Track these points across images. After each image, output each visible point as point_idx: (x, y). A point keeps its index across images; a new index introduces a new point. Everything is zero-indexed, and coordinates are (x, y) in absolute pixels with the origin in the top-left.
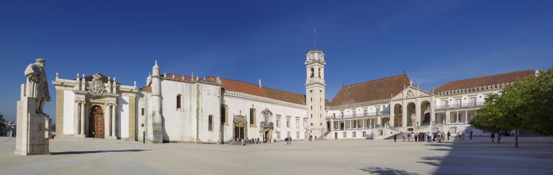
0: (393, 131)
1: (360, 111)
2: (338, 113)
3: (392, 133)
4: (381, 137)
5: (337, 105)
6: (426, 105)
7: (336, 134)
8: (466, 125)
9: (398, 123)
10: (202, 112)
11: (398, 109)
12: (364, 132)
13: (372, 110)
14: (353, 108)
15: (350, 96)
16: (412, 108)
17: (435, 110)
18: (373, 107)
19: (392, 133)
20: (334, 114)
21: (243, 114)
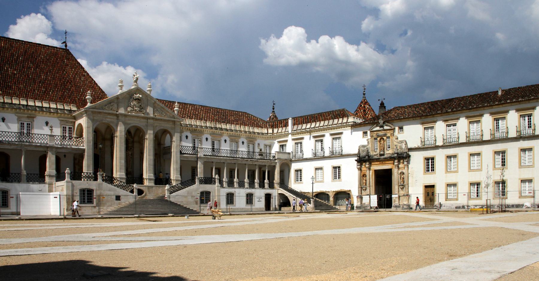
19: (118, 198)
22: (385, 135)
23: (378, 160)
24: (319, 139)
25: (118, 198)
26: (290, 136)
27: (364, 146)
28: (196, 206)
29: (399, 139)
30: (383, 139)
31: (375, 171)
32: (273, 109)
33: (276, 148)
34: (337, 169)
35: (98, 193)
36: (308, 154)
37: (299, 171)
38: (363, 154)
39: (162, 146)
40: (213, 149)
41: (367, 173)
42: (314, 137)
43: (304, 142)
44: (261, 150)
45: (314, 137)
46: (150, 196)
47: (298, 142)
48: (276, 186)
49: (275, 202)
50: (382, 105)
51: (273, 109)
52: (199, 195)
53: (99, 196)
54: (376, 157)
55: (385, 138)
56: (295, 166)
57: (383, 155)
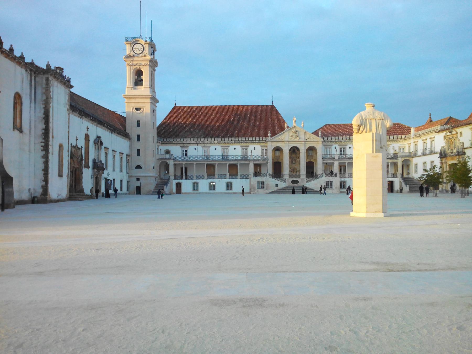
2: (176, 150)
7: (179, 186)
9: (277, 171)
10: (53, 137)
13: (235, 150)
18: (238, 147)
19: (277, 185)
20: (168, 152)
21: (79, 146)
22: (453, 138)
23: (450, 156)
25: (277, 185)
27: (443, 146)
29: (461, 141)
31: (451, 165)
33: (407, 150)
36: (420, 153)
37: (416, 164)
38: (442, 152)
41: (445, 165)
42: (423, 140)
45: (423, 140)
46: (301, 184)
49: (396, 187)
51: (430, 115)
52: (325, 183)
53: (267, 185)
54: (449, 155)
55: (453, 140)
56: (415, 160)
57: (452, 153)
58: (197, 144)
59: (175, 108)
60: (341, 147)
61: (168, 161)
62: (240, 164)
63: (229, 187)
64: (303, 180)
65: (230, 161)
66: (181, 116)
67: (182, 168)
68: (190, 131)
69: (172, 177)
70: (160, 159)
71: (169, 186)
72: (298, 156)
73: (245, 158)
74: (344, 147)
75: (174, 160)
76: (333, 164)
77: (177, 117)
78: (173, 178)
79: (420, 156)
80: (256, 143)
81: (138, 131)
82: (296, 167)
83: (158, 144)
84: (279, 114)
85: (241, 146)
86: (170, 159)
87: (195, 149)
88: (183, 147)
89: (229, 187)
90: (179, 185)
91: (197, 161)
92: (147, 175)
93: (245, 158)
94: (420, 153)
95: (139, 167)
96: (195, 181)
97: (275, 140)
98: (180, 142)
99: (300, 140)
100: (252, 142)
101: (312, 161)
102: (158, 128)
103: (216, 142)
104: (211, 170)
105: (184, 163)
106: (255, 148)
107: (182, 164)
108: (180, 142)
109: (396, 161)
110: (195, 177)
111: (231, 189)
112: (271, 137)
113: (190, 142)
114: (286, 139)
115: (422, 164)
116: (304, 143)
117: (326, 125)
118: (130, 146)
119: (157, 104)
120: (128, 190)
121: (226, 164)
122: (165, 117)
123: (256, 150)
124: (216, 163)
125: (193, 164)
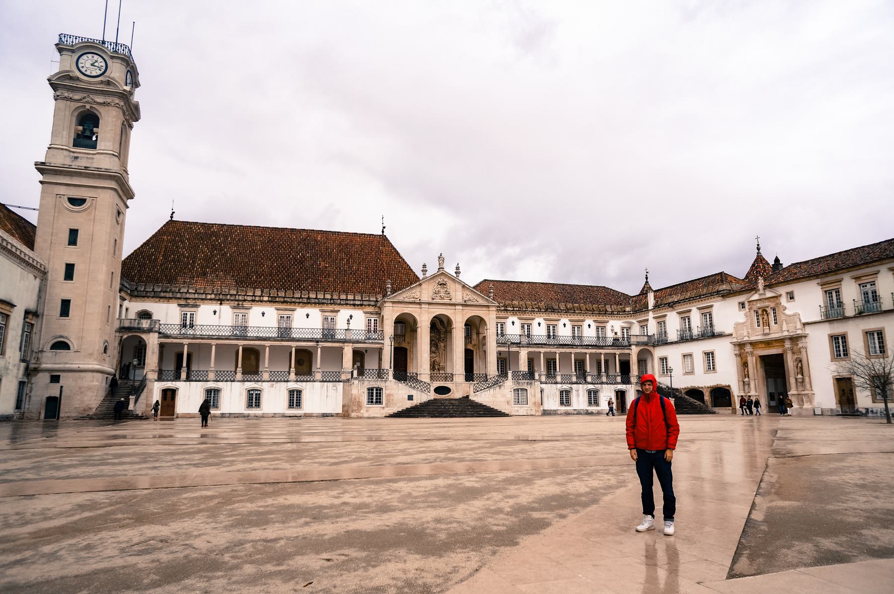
0: (413, 392)
1: (263, 319)
2: (167, 314)
3: (410, 398)
4: (376, 410)
5: (157, 281)
6: (473, 326)
7: (169, 396)
8: (559, 386)
11: (406, 326)
12: (291, 392)
13: (307, 321)
14: (239, 304)
15: (207, 259)
16: (441, 328)
17: (499, 344)
19: (410, 398)
20: (145, 315)
24: (685, 317)
26: (651, 314)
28: (507, 407)
30: (766, 311)
32: (647, 278)
33: (636, 330)
34: (709, 356)
35: (388, 392)
36: (673, 336)
37: (664, 360)
39: (481, 336)
40: (549, 336)
43: (667, 319)
44: (616, 333)
45: (679, 313)
47: (661, 323)
48: (634, 380)
50: (777, 260)
51: (647, 278)
53: (388, 395)
58: (221, 302)
59: (171, 221)
60: (523, 321)
61: (144, 336)
62: (322, 348)
63: (295, 399)
64: (459, 388)
65: (299, 340)
66: (182, 242)
67: (180, 356)
68: (205, 274)
69: (152, 376)
70: (122, 329)
71: (143, 396)
72: (442, 336)
73: (328, 334)
74: (529, 322)
75: (160, 333)
76: (518, 353)
77: (174, 242)
78: (155, 376)
79: (676, 343)
80: (354, 305)
81: (71, 255)
82: (437, 359)
83: (123, 294)
84: (398, 253)
85: (323, 311)
86: (150, 331)
87: (215, 312)
88: (186, 306)
89: (295, 399)
90: (169, 394)
91: (219, 338)
92: (82, 367)
93: (328, 334)
94: (673, 336)
95: (61, 345)
96: (211, 385)
97: (400, 298)
98: (179, 295)
99: (453, 301)
100: (346, 304)
101: (470, 347)
102: (124, 263)
103: (266, 299)
104: (250, 360)
105: (186, 341)
106: (351, 317)
107: (182, 345)
108: (179, 295)
109: (627, 351)
110: (212, 376)
111: (299, 405)
112: (394, 291)
113: (204, 296)
114: (426, 298)
115: (680, 358)
116: (461, 307)
117: (485, 280)
118: (42, 291)
119: (129, 202)
120: (18, 406)
121: (291, 347)
122: (145, 241)
123: (352, 321)
124: (267, 343)
125: (210, 346)
